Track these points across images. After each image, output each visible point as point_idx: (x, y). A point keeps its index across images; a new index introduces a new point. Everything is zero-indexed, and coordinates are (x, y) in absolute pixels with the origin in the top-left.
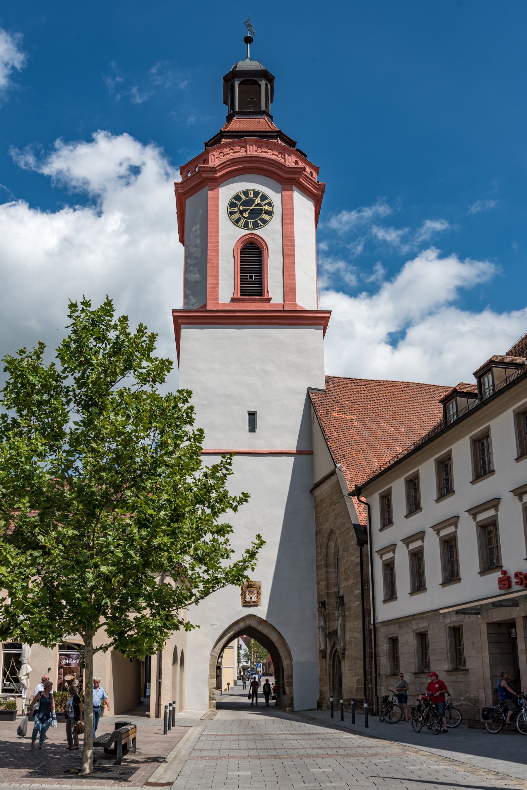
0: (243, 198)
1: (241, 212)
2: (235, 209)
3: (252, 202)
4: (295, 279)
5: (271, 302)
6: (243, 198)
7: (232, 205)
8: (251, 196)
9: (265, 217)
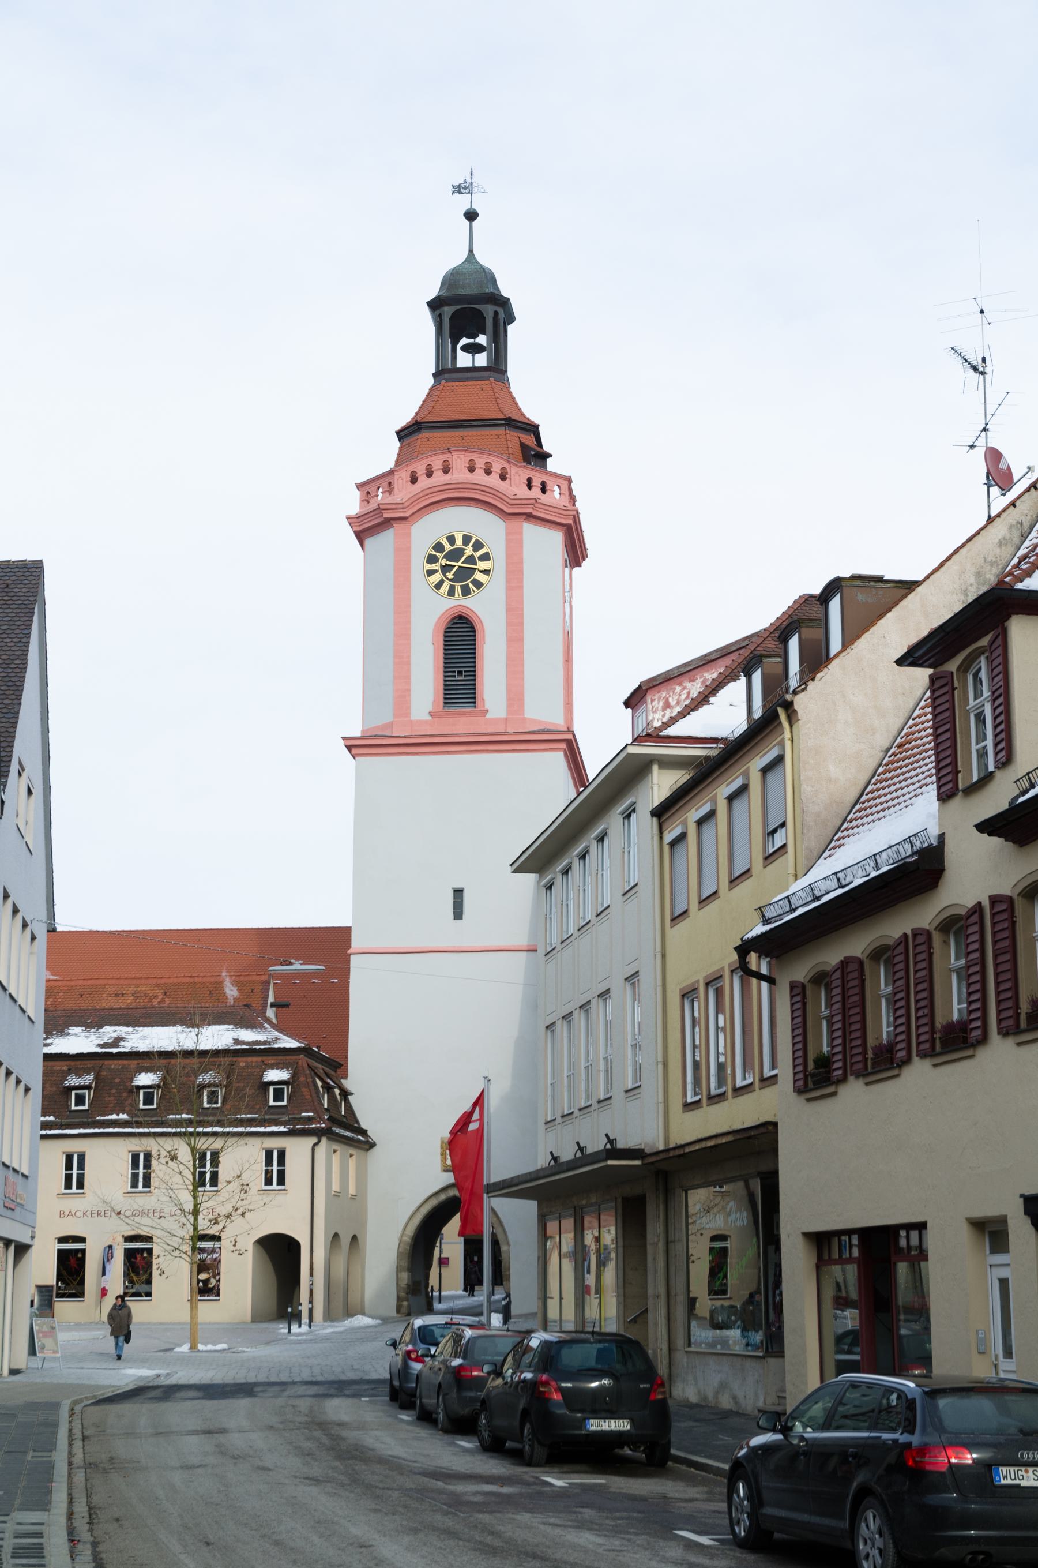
0: (448, 547)
1: (446, 569)
2: (436, 566)
3: (460, 552)
4: (523, 679)
5: (488, 716)
6: (448, 547)
7: (432, 559)
8: (459, 543)
9: (478, 576)
